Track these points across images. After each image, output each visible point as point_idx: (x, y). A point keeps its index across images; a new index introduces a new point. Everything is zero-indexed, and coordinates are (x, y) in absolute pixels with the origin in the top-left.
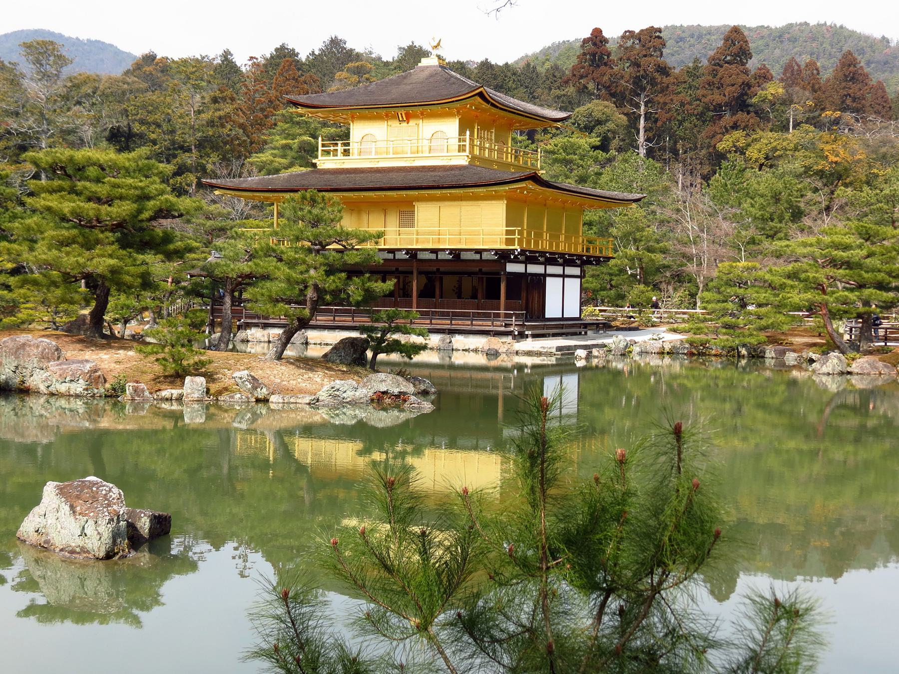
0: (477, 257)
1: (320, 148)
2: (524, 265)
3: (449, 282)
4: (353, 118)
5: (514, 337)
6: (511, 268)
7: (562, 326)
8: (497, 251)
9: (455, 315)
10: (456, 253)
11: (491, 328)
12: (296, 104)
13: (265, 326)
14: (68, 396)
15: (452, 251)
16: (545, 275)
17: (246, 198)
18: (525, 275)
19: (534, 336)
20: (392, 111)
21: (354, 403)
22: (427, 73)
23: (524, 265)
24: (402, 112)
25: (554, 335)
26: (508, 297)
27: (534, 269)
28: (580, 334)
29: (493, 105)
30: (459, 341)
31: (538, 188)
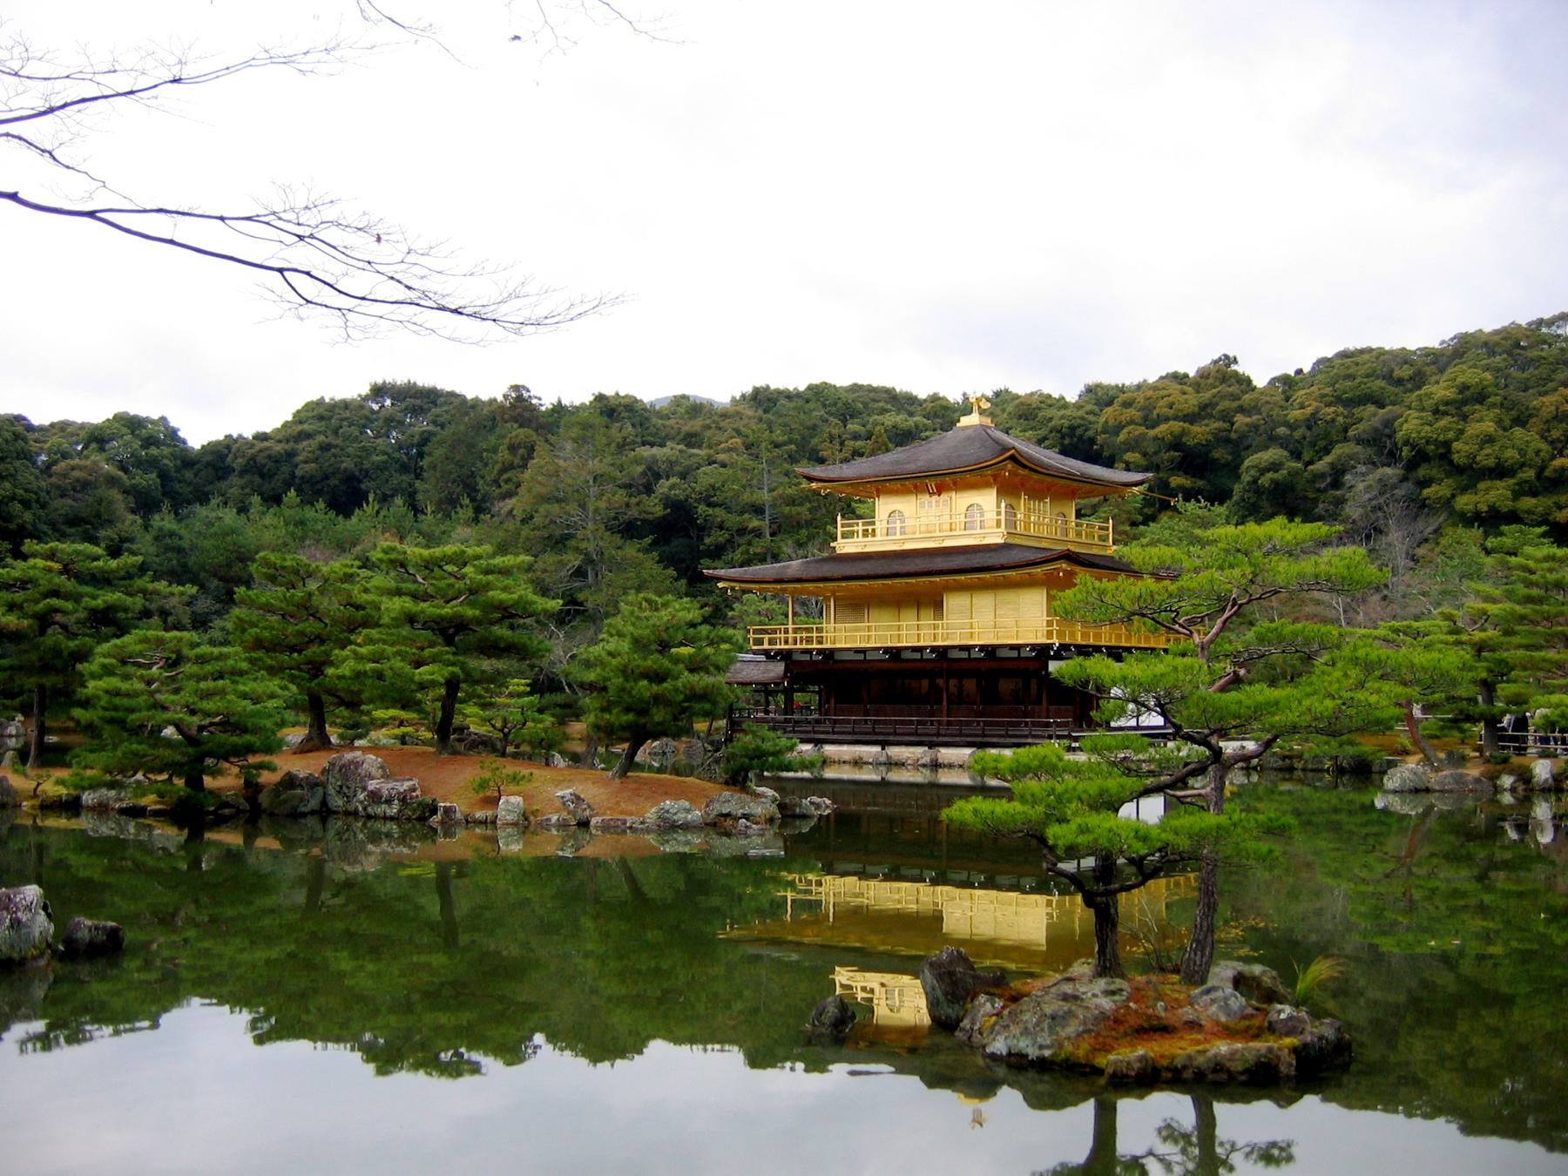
0: (1014, 654)
3: (1006, 686)
4: (879, 493)
8: (1034, 647)
10: (990, 650)
12: (810, 479)
14: (386, 818)
15: (983, 648)
17: (793, 593)
20: (918, 482)
21: (686, 827)
22: (963, 435)
24: (932, 485)
26: (1050, 703)
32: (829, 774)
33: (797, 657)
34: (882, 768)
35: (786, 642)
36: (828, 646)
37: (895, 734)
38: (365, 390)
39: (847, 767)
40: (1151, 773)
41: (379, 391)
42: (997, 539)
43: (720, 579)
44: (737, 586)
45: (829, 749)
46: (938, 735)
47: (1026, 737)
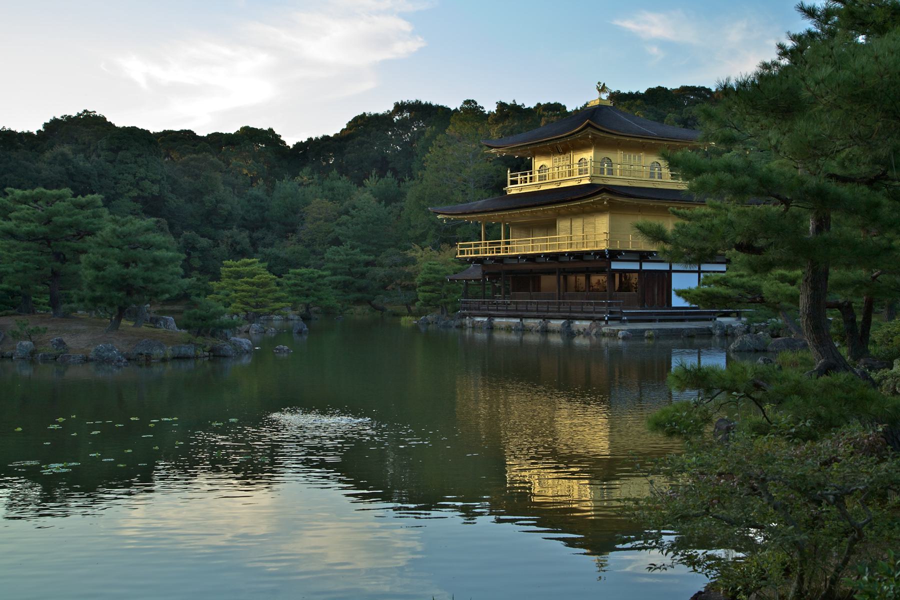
1: (509, 179)
2: (638, 264)
5: (607, 323)
6: (615, 266)
7: (681, 314)
9: (597, 304)
10: (579, 256)
11: (595, 315)
12: (492, 148)
13: (471, 316)
16: (670, 272)
18: (640, 272)
19: (631, 321)
23: (638, 264)
25: (660, 321)
27: (647, 266)
28: (711, 320)
29: (607, 132)
30: (579, 325)
31: (619, 199)
32: (498, 336)
33: (486, 263)
34: (520, 333)
35: (477, 252)
36: (495, 254)
37: (527, 311)
38: (391, 108)
39: (503, 332)
40: (650, 338)
41: (400, 108)
42: (586, 182)
43: (439, 214)
44: (452, 217)
45: (497, 320)
46: (548, 311)
47: (591, 312)
